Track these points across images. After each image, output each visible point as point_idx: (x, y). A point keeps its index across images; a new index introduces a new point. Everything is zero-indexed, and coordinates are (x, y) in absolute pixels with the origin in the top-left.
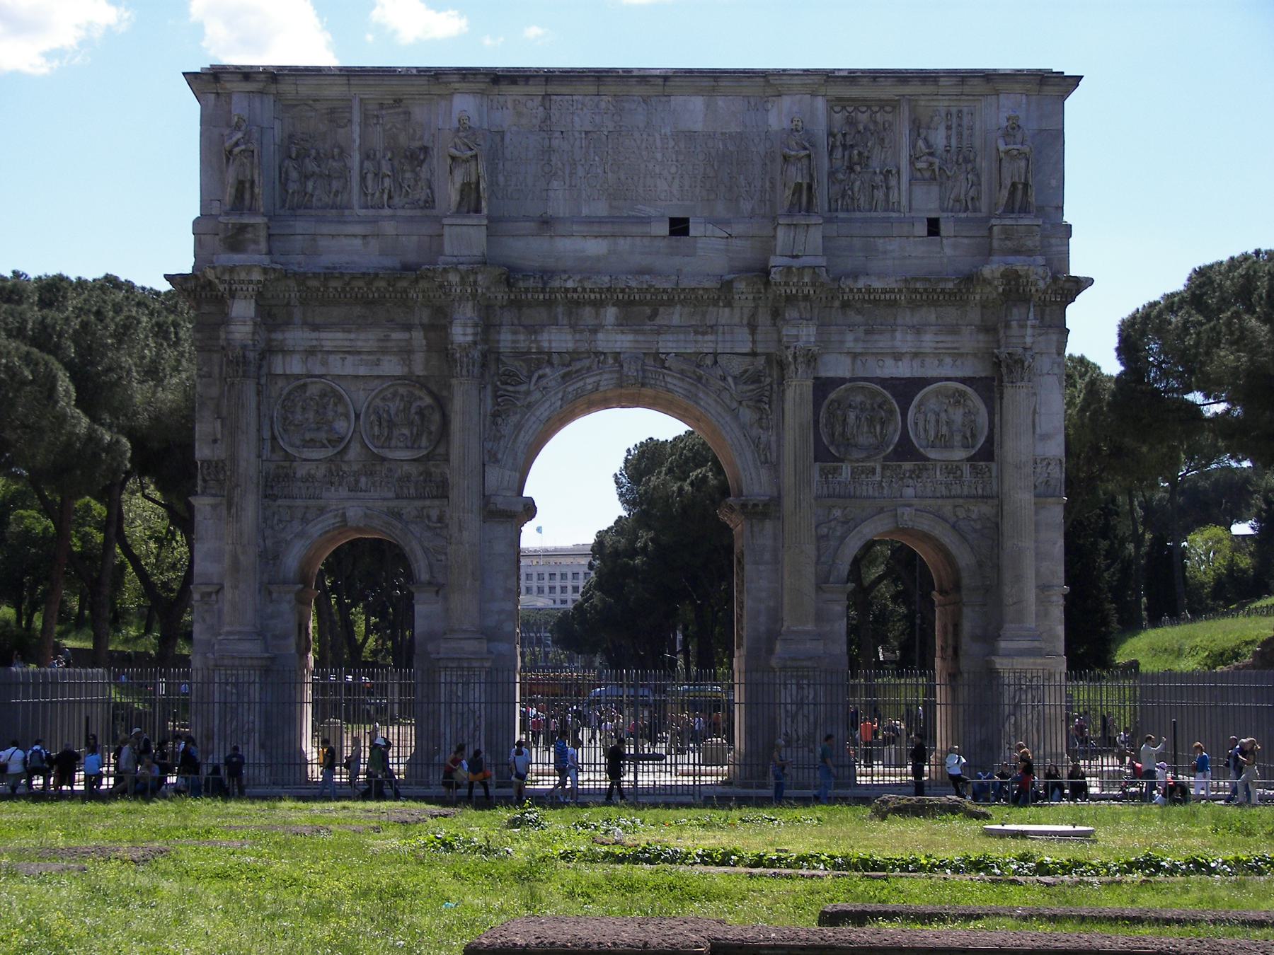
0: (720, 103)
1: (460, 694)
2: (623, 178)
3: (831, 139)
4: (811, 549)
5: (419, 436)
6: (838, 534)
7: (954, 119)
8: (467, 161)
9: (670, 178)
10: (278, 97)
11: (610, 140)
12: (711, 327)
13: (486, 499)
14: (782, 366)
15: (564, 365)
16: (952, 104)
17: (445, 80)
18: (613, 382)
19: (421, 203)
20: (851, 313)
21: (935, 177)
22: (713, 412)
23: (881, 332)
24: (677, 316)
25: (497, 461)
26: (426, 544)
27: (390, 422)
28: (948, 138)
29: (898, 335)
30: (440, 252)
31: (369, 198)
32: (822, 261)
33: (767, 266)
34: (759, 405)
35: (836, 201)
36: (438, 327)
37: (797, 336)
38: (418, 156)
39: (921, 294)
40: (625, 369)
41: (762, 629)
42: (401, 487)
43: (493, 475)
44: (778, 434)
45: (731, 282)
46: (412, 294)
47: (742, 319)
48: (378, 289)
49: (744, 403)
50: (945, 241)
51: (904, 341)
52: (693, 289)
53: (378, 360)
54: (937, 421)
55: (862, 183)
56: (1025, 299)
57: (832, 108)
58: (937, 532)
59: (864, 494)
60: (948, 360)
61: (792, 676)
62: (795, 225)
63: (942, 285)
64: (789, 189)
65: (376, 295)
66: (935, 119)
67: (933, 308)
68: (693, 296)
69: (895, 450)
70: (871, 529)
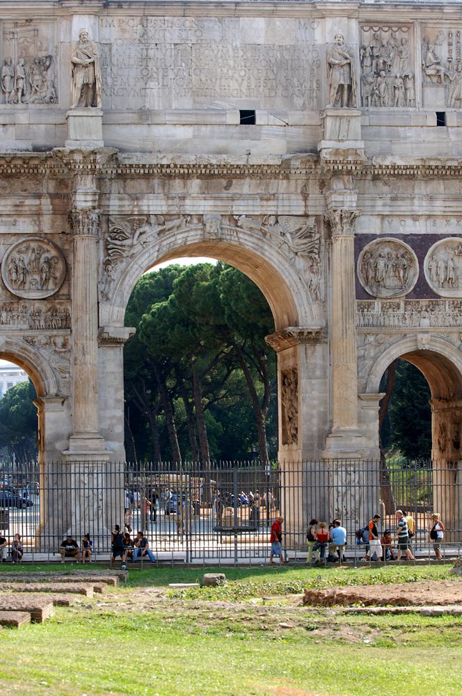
0: (278, 23)
1: (86, 482)
2: (204, 79)
3: (362, 51)
4: (353, 366)
5: (47, 280)
6: (372, 354)
7: (454, 38)
8: (86, 67)
9: (240, 80)
11: (193, 51)
12: (274, 195)
13: (101, 329)
14: (329, 225)
15: (159, 224)
16: (452, 26)
17: (67, 5)
18: (198, 237)
19: (47, 99)
20: (380, 184)
21: (442, 80)
22: (275, 260)
23: (403, 199)
24: (246, 187)
25: (108, 299)
26: (53, 365)
28: (450, 51)
29: (416, 202)
30: (66, 136)
31: (7, 95)
32: (360, 144)
33: (316, 148)
34: (310, 255)
35: (367, 98)
36: (63, 195)
37: (343, 202)
38: (44, 64)
39: (433, 170)
40: (208, 225)
41: (315, 429)
42: (34, 320)
43: (105, 310)
44: (325, 278)
45: (289, 159)
46: (42, 170)
47: (296, 188)
48: (15, 166)
49: (299, 254)
50: (449, 129)
51: (420, 207)
52: (260, 166)
53: (15, 221)
54: (446, 268)
55: (387, 85)
57: (362, 28)
58: (446, 353)
59: (392, 323)
60: (454, 221)
61: (342, 465)
62: (341, 117)
63: (449, 164)
64: (335, 88)
65: (14, 171)
66: (441, 37)
67: (442, 181)
68: (259, 171)
69: (414, 289)
70: (397, 351)
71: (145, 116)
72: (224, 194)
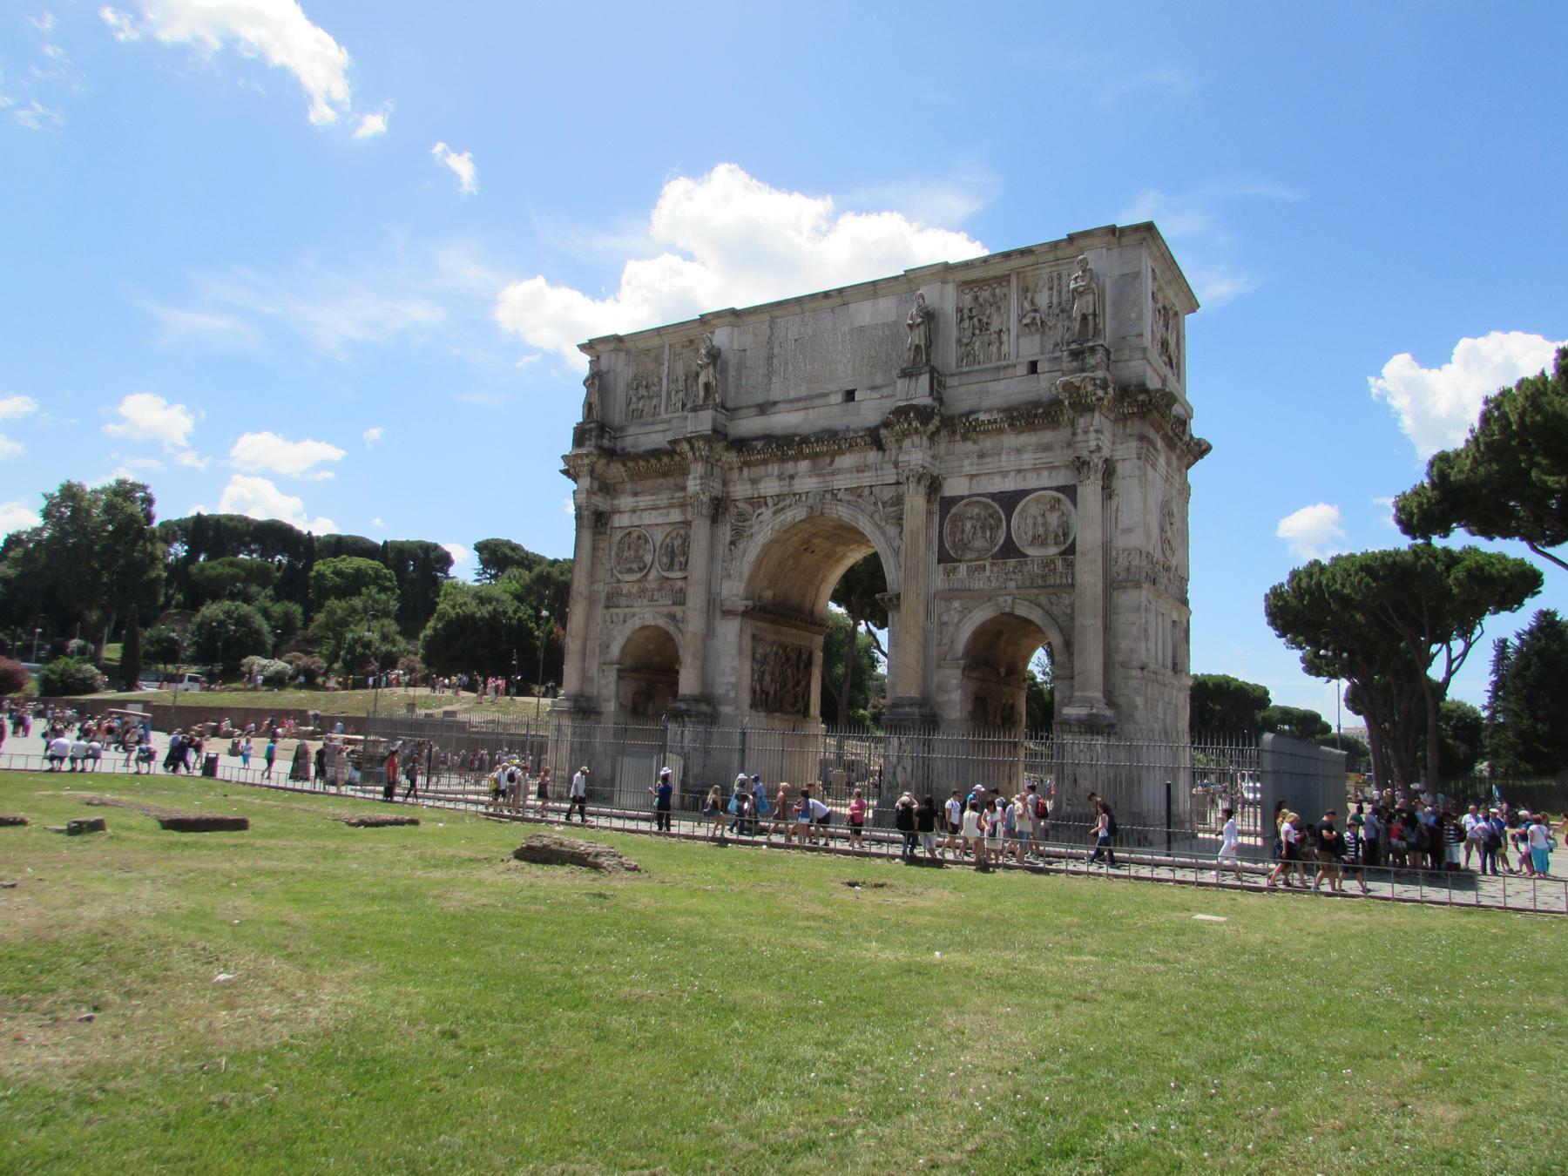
6: (956, 620)
7: (1055, 281)
10: (628, 352)
24: (846, 461)
25: (729, 576)
27: (673, 552)
28: (1051, 296)
29: (1004, 457)
32: (928, 401)
45: (877, 428)
54: (1035, 524)
56: (1090, 409)
59: (976, 587)
60: (1045, 473)
66: (1040, 284)
69: (1001, 550)
70: (982, 615)
71: (763, 408)
72: (829, 470)
